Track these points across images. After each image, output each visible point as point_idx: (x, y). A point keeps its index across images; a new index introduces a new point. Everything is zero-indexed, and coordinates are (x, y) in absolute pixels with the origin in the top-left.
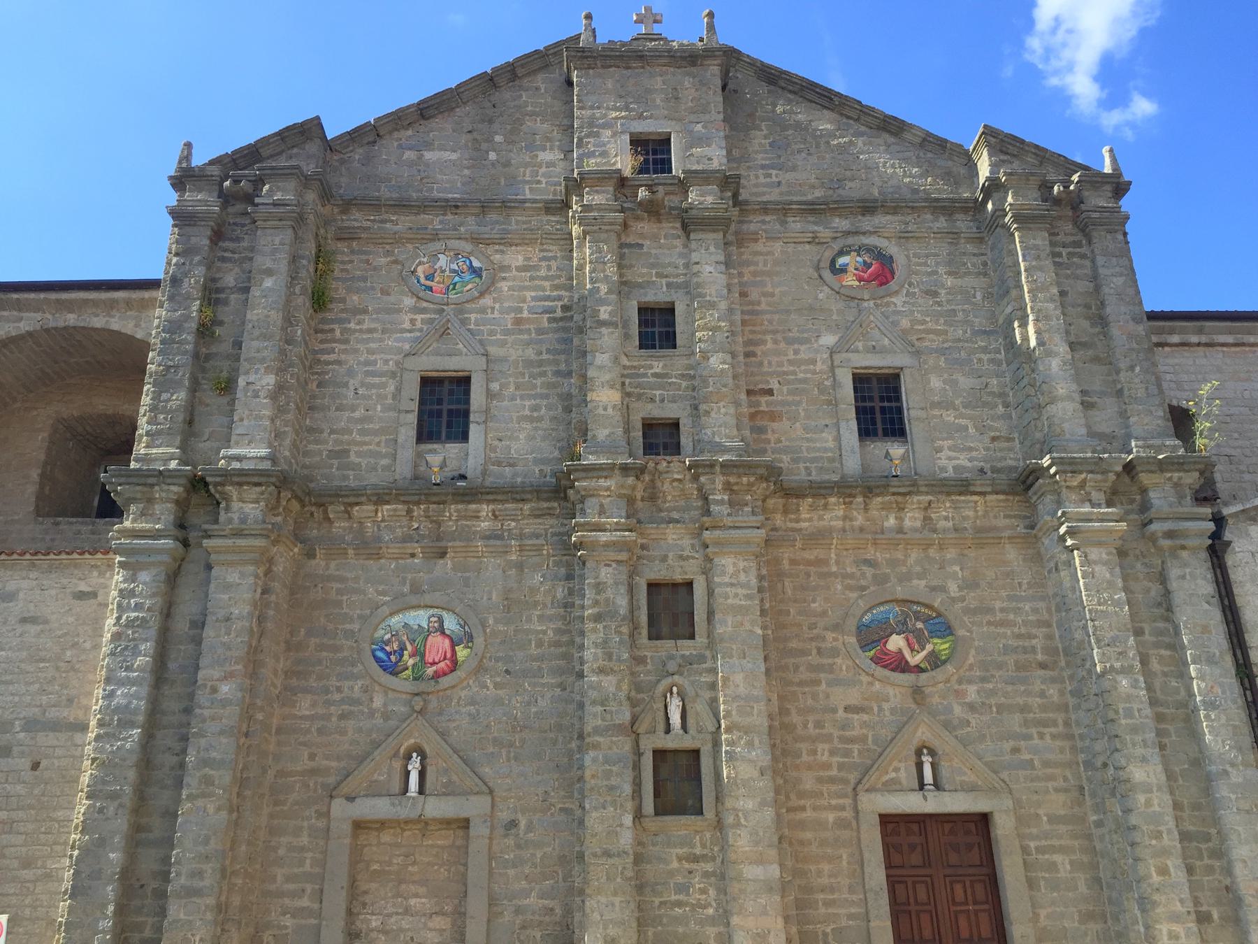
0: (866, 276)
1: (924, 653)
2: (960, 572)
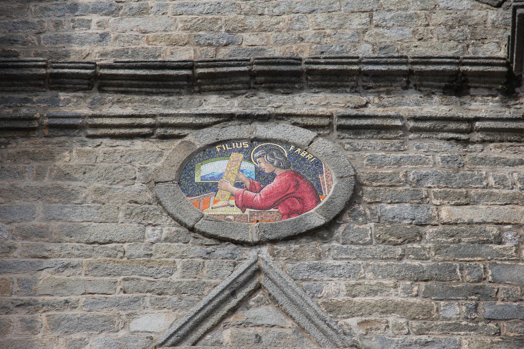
0: (258, 197)
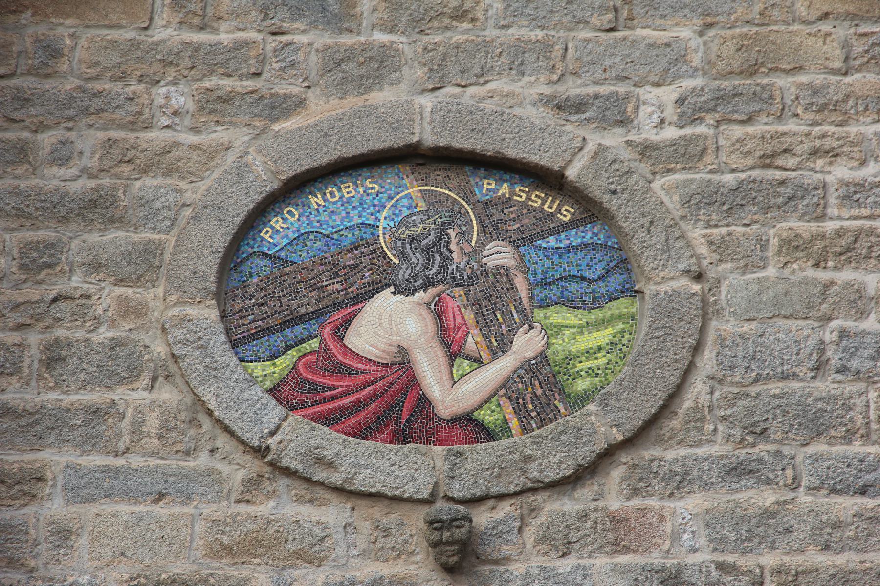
1: (504, 365)
2: (696, 42)
